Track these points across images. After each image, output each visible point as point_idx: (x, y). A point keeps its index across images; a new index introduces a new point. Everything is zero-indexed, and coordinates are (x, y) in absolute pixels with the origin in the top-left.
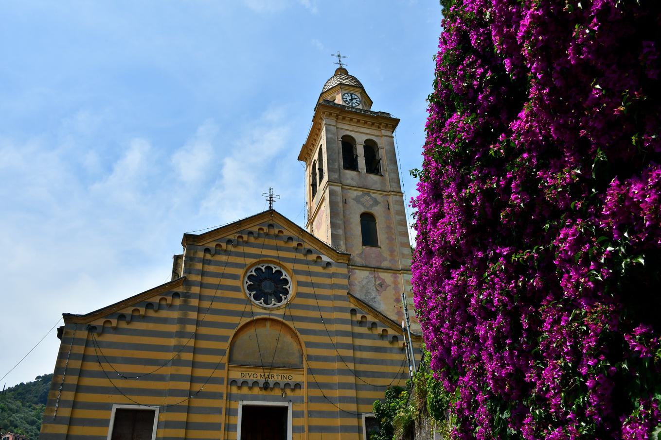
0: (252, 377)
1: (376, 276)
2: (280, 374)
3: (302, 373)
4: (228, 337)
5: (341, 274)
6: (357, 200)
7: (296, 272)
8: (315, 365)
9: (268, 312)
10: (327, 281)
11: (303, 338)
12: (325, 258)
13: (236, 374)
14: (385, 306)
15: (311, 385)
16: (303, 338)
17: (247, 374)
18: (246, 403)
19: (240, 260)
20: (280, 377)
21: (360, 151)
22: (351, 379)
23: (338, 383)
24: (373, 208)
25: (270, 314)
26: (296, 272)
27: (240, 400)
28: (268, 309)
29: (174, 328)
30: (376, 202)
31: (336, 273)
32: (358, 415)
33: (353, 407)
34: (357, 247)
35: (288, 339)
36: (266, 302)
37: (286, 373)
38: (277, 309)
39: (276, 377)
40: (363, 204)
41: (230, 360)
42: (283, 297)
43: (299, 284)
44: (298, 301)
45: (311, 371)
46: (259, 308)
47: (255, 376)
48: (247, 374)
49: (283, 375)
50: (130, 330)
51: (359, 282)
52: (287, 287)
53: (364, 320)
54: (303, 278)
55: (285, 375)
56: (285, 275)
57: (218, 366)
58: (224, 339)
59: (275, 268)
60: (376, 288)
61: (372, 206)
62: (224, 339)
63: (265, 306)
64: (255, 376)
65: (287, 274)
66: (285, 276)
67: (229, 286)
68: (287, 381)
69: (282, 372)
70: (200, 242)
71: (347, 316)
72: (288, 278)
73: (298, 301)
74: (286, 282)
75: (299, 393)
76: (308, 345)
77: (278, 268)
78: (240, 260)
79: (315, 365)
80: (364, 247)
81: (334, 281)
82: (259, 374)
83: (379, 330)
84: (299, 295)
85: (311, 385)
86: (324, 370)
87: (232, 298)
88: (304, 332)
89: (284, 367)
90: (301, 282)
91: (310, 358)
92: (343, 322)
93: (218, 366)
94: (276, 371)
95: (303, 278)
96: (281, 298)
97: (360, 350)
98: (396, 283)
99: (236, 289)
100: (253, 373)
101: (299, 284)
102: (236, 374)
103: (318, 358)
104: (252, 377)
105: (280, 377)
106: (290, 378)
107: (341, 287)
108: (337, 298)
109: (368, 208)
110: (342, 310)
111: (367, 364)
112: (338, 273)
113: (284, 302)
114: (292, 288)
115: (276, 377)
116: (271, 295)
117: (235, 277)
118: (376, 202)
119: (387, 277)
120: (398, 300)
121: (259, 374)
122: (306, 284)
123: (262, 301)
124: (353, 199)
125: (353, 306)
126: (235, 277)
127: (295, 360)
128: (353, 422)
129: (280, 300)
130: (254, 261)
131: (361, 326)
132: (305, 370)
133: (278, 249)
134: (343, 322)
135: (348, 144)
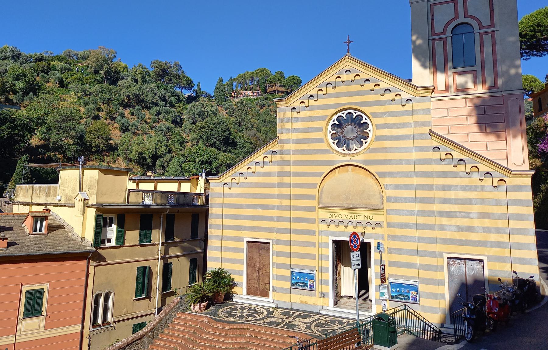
0: (337, 218)
4: (317, 184)
7: (375, 115)
9: (349, 159)
10: (408, 119)
25: (350, 161)
26: (375, 115)
35: (370, 180)
36: (349, 149)
37: (367, 213)
38: (359, 154)
39: (358, 217)
41: (318, 203)
42: (364, 141)
45: (389, 212)
47: (340, 216)
52: (367, 131)
55: (366, 215)
57: (311, 209)
58: (313, 186)
59: (356, 113)
62: (313, 186)
63: (347, 152)
64: (340, 216)
66: (366, 119)
68: (368, 220)
77: (359, 113)
82: (343, 215)
88: (383, 174)
89: (365, 208)
91: (389, 199)
93: (311, 209)
96: (362, 142)
99: (320, 141)
100: (339, 214)
101: (379, 127)
102: (324, 214)
104: (337, 218)
105: (361, 217)
106: (371, 218)
107: (424, 124)
108: (415, 137)
114: (372, 132)
115: (358, 217)
121: (343, 215)
123: (344, 148)
127: (376, 201)
129: (361, 144)
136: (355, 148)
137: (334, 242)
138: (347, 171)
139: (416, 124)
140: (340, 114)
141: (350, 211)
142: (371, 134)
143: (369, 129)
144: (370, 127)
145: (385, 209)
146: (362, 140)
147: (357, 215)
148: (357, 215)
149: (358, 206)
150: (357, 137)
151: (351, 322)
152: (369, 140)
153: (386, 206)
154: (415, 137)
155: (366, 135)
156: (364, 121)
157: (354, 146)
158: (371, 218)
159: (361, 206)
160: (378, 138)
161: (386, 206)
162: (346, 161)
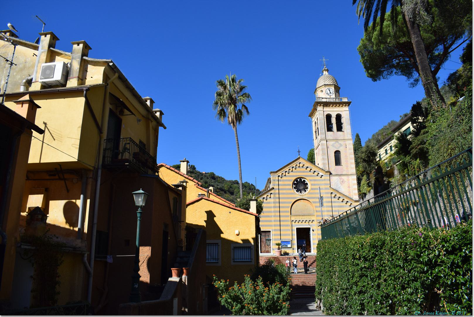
6: (333, 145)
12: (321, 174)
13: (293, 218)
14: (344, 190)
19: (290, 178)
21: (334, 121)
26: (311, 180)
29: (273, 205)
30: (341, 145)
34: (333, 168)
38: (304, 195)
43: (312, 185)
44: (312, 191)
46: (298, 195)
54: (313, 182)
56: (307, 181)
58: (288, 207)
61: (339, 147)
73: (312, 191)
74: (307, 184)
78: (290, 178)
83: (341, 200)
84: (312, 189)
95: (313, 182)
98: (348, 180)
113: (307, 192)
114: (309, 186)
117: (289, 185)
118: (341, 145)
119: (345, 178)
120: (349, 187)
126: (289, 185)
129: (305, 191)
133: (304, 172)
135: (329, 117)
137: (297, 229)
157: (303, 192)
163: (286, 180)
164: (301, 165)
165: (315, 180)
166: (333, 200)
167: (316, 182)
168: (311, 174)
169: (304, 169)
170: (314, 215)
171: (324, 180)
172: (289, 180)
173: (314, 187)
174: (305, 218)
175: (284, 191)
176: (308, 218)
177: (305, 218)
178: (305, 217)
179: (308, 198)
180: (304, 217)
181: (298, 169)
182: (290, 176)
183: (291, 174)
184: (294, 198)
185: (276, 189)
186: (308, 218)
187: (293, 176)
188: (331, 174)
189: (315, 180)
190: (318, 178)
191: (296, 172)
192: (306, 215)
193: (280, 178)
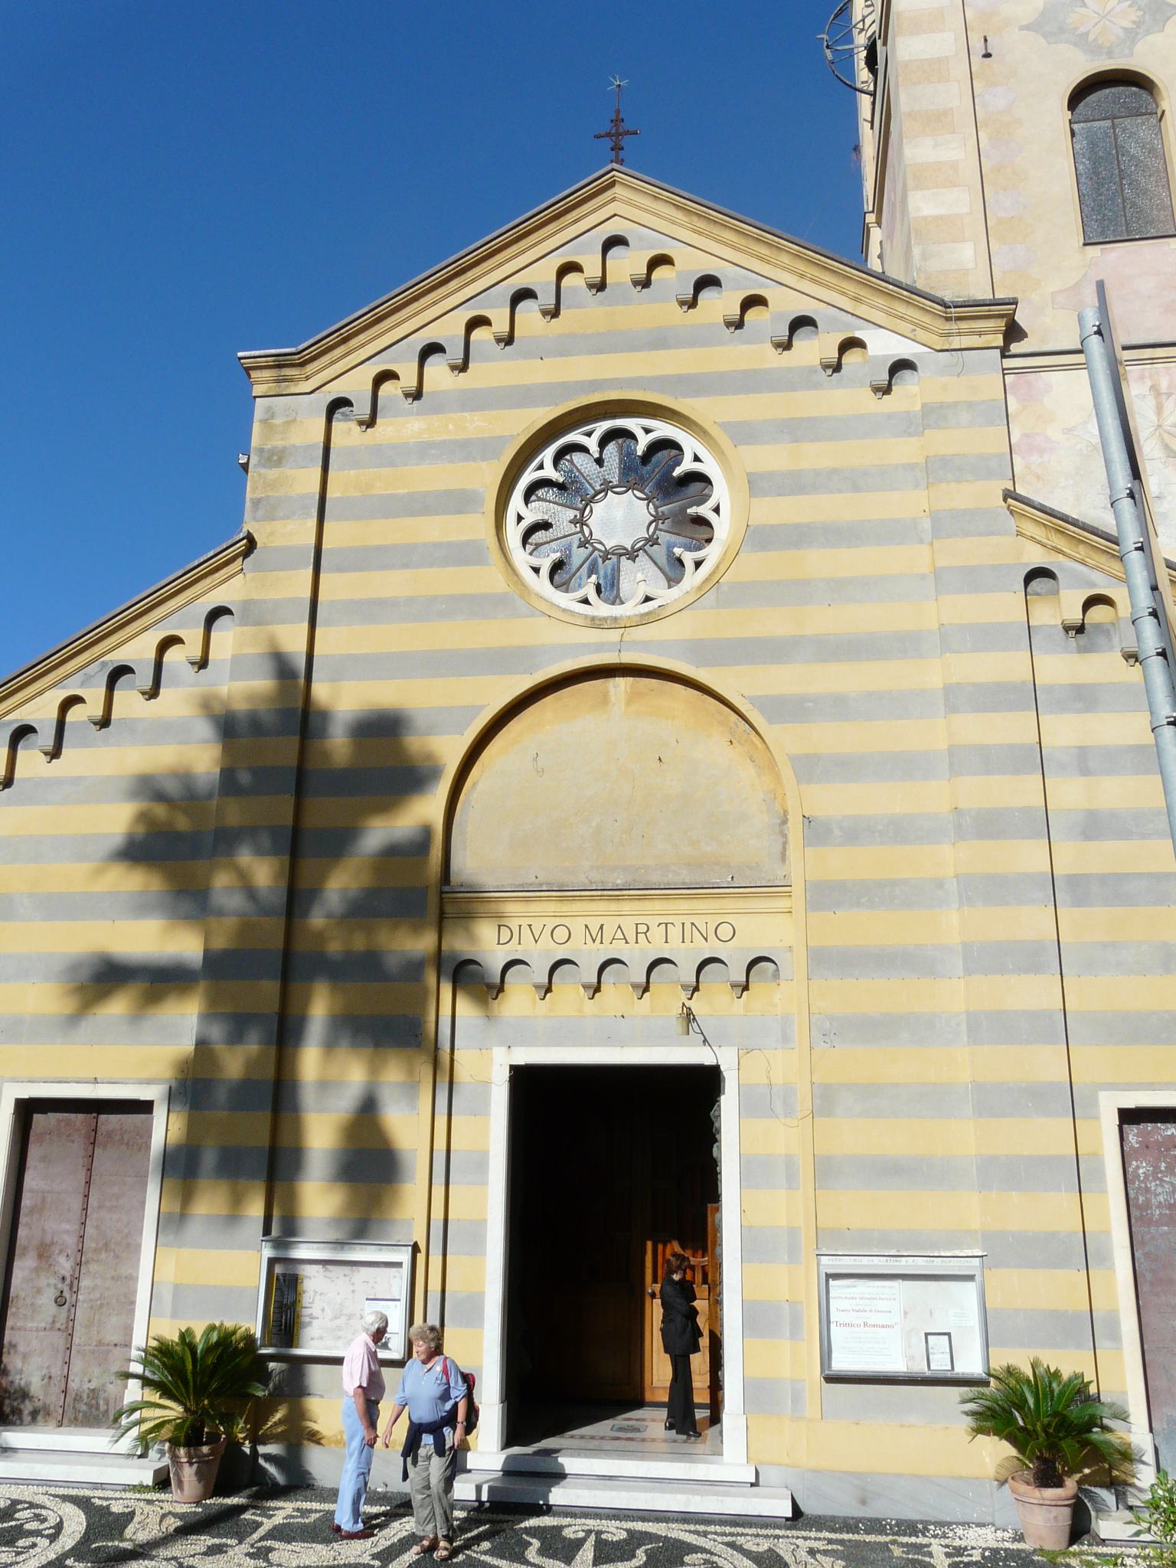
1: (1164, 385)
2: (677, 920)
3: (782, 904)
5: (970, 405)
7: (745, 433)
8: (839, 863)
9: (614, 636)
10: (906, 450)
11: (783, 738)
15: (825, 961)
16: (783, 738)
17: (525, 931)
18: (526, 1056)
19: (476, 424)
20: (675, 932)
22: (1033, 922)
23: (965, 944)
24: (1140, 47)
26: (745, 433)
27: (501, 1045)
28: (614, 623)
31: (942, 406)
32: (1074, 1103)
33: (1046, 1064)
37: (703, 912)
39: (657, 933)
40: (1082, 41)
43: (756, 485)
44: (754, 566)
47: (561, 934)
48: (525, 931)
49: (688, 921)
50: (59, 782)
51: (1068, 431)
53: (1098, 613)
55: (700, 922)
60: (1166, 447)
61: (1132, 36)
63: (601, 609)
64: (561, 934)
65: (703, 453)
67: (438, 545)
69: (684, 905)
70: (307, 378)
71: (1009, 604)
72: (708, 466)
73: (754, 566)
75: (771, 998)
76: (810, 768)
78: (476, 424)
79: (839, 863)
80: (1094, 251)
81: (943, 442)
82: (577, 926)
84: (759, 538)
85: (825, 961)
86: (893, 883)
87: (452, 598)
90: (770, 475)
91: (816, 831)
92: (985, 637)
94: (657, 906)
96: (680, 562)
97: (1085, 771)
100: (551, 923)
101: (756, 485)
103: (855, 833)
105: (675, 932)
106: (725, 931)
108: (945, 524)
109: (1110, 54)
110: (972, 579)
111: (1124, 834)
112: (955, 405)
113: (692, 579)
115: (657, 933)
116: (632, 555)
117: (459, 502)
121: (577, 926)
122: (793, 484)
124: (1022, 28)
125: (1037, 557)
126: (459, 502)
128: (1050, 1135)
130: (542, 415)
131: (1083, 650)
132: (798, 889)
133: (660, 340)
134: (985, 637)
136: (642, 591)
138: (605, 699)
139: (937, 470)
140: (574, 437)
141: (613, 906)
142: (723, 528)
143: (711, 503)
144: (720, 492)
145: (798, 889)
146: (677, 551)
147: (653, 922)
148: (653, 922)
149: (655, 878)
150: (652, 541)
151: (615, 1531)
152: (712, 554)
153: (804, 865)
154: (945, 524)
155: (702, 532)
156: (687, 465)
158: (725, 931)
159: (671, 878)
160: (759, 538)
161: (804, 865)
162: (599, 647)
163: (425, 451)
164: (627, 264)
165: (797, 430)
166: (1061, 666)
167: (815, 456)
168: (753, 352)
169: (660, 309)
170: (776, 888)
171: (933, 415)
172: (467, 450)
173: (774, 511)
174: (641, 931)
175: (392, 584)
176: (675, 931)
177: (641, 931)
178: (652, 912)
179: (700, 650)
180: (627, 914)
181: (584, 312)
182: (472, 401)
183: (492, 370)
184: (498, 660)
185: (285, 560)
186: (675, 931)
187: (522, 397)
188: (1013, 332)
189: (797, 430)
190: (848, 397)
191: (564, 348)
192: (668, 890)
193: (345, 431)
